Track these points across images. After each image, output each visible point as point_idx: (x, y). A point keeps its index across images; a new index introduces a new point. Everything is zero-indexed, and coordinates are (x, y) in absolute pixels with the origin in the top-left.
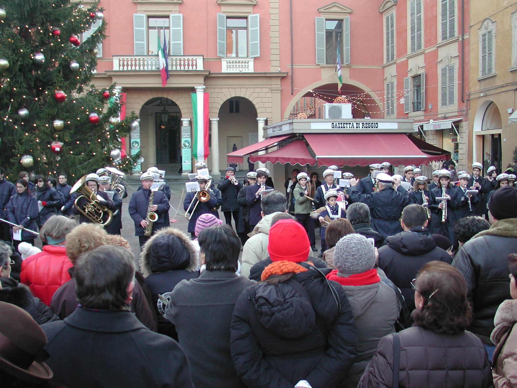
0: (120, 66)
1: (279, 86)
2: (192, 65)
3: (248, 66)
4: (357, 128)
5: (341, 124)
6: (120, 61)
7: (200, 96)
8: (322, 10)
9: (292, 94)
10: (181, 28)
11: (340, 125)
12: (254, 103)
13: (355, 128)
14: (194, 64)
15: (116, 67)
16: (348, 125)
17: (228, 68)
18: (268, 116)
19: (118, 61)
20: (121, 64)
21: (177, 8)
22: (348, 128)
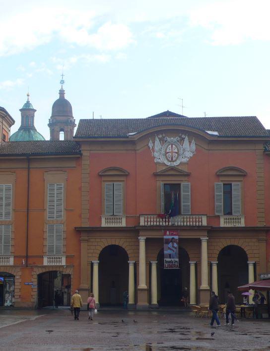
0: (145, 222)
2: (199, 222)
6: (145, 218)
7: (204, 245)
10: (190, 193)
15: (142, 223)
18: (257, 260)
19: (143, 218)
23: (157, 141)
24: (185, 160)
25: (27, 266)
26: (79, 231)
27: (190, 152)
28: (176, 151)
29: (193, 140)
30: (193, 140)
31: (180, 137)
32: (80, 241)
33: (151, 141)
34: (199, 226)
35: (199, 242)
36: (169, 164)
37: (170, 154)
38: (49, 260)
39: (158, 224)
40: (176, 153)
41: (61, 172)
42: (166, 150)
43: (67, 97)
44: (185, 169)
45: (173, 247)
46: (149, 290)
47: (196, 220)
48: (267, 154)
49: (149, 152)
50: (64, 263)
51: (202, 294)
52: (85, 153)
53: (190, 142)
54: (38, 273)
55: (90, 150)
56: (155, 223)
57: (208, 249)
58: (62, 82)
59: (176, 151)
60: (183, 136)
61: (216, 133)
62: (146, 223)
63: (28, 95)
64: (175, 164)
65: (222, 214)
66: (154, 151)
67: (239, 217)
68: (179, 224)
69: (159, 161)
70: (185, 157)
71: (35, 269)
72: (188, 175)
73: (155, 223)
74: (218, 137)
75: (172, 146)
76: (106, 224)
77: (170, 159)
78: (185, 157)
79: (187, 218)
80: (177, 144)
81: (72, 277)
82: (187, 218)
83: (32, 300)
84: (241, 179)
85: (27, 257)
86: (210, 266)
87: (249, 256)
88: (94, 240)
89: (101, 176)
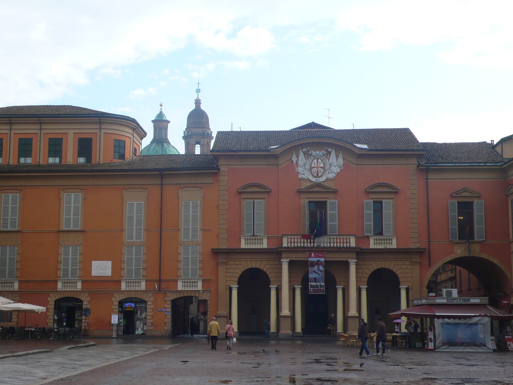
0: (288, 243)
1: (418, 260)
2: (347, 243)
3: (392, 242)
4: (459, 301)
5: (452, 300)
6: (288, 239)
7: (353, 268)
8: (455, 195)
9: (430, 266)
10: (337, 212)
11: (451, 300)
12: (397, 273)
13: (459, 302)
14: (348, 242)
15: (285, 245)
16: (455, 300)
17: (374, 244)
19: (286, 239)
20: (289, 242)
21: (333, 196)
22: (455, 302)
23: (301, 155)
24: (331, 176)
25: (160, 291)
26: (216, 253)
27: (337, 167)
28: (322, 165)
29: (341, 155)
30: (341, 154)
31: (326, 150)
32: (217, 264)
33: (294, 156)
34: (347, 248)
35: (346, 264)
36: (314, 180)
37: (316, 169)
38: (184, 284)
39: (302, 245)
40: (322, 168)
41: (198, 189)
42: (311, 164)
43: (203, 107)
44: (332, 185)
45: (319, 270)
46: (293, 317)
47: (343, 241)
48: (421, 169)
49: (292, 167)
50: (200, 287)
51: (350, 322)
52: (223, 169)
53: (337, 156)
54: (172, 298)
55: (229, 165)
56: (299, 244)
57: (357, 273)
58: (198, 91)
59: (322, 165)
60: (330, 150)
61: (365, 146)
62: (289, 244)
63: (161, 105)
64: (321, 180)
65: (372, 234)
66: (298, 166)
67: (391, 238)
68: (325, 245)
69: (304, 176)
70: (332, 172)
71: (168, 294)
72: (335, 192)
73: (299, 244)
74: (368, 150)
75: (317, 161)
76: (246, 245)
77: (316, 175)
78: (332, 172)
79: (334, 239)
80: (322, 159)
81: (209, 302)
82: (334, 239)
83: (166, 328)
84: (393, 196)
85: (160, 281)
86: (359, 291)
87: (401, 280)
88: (232, 263)
89: (240, 193)
